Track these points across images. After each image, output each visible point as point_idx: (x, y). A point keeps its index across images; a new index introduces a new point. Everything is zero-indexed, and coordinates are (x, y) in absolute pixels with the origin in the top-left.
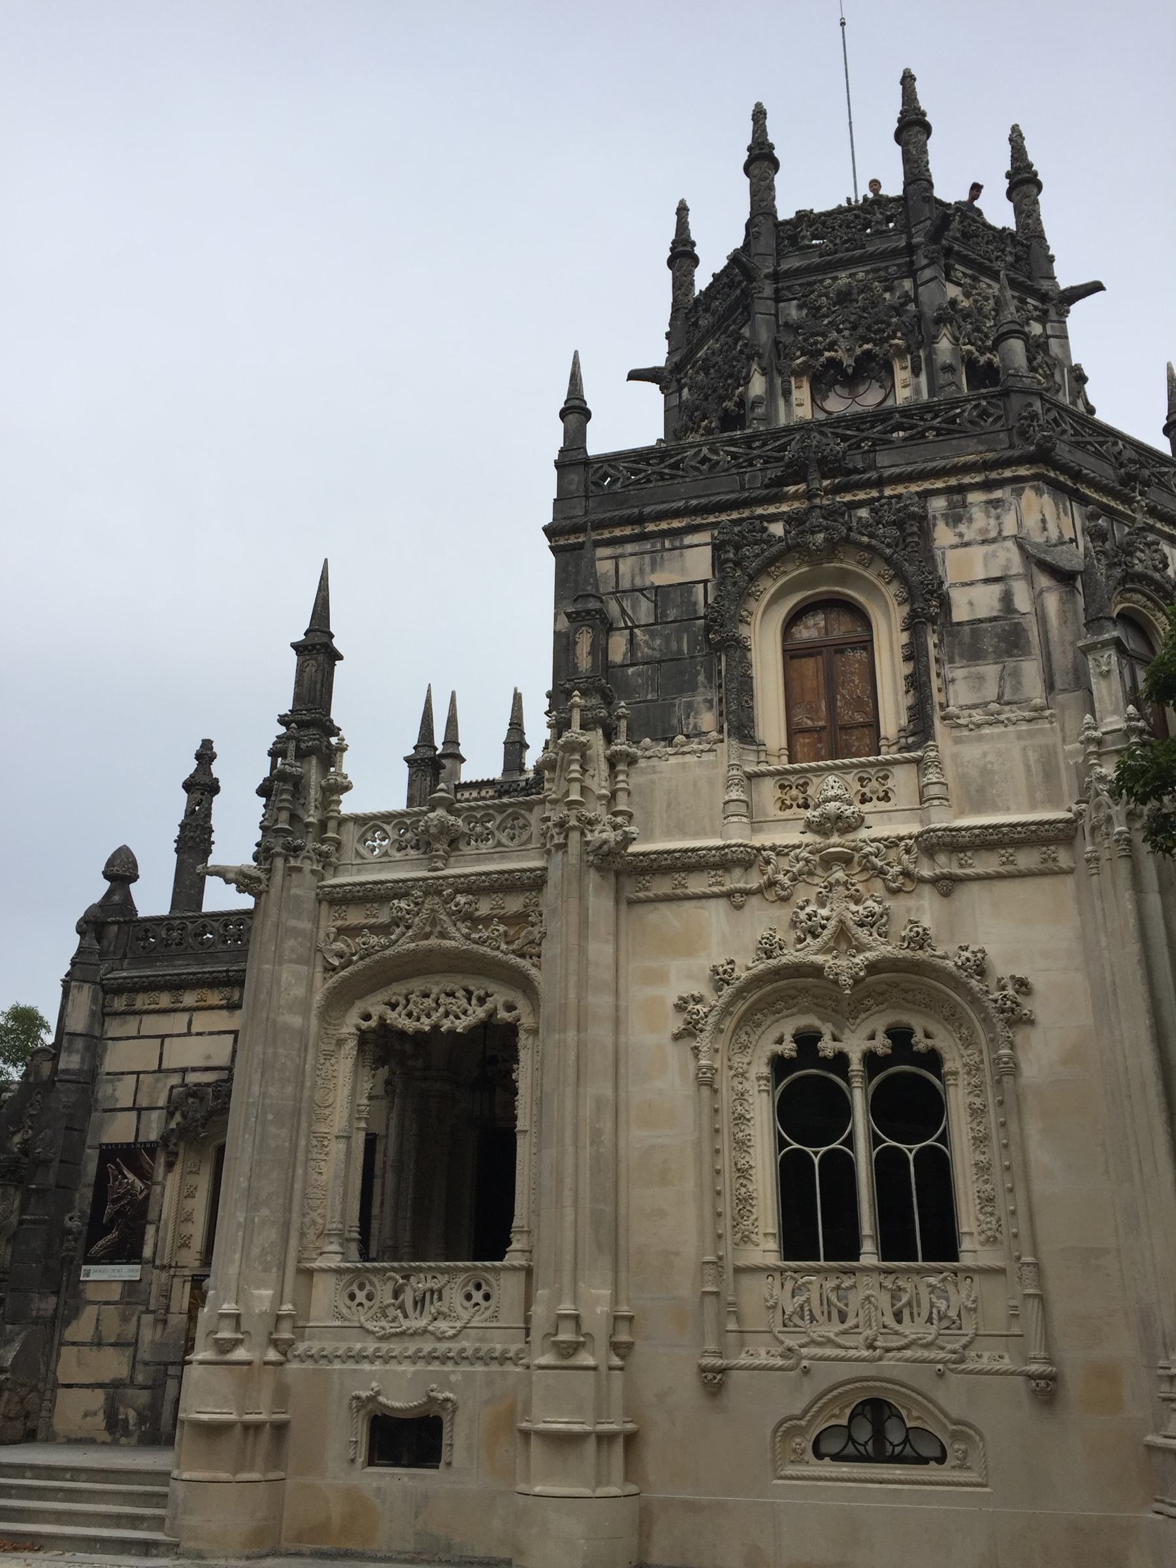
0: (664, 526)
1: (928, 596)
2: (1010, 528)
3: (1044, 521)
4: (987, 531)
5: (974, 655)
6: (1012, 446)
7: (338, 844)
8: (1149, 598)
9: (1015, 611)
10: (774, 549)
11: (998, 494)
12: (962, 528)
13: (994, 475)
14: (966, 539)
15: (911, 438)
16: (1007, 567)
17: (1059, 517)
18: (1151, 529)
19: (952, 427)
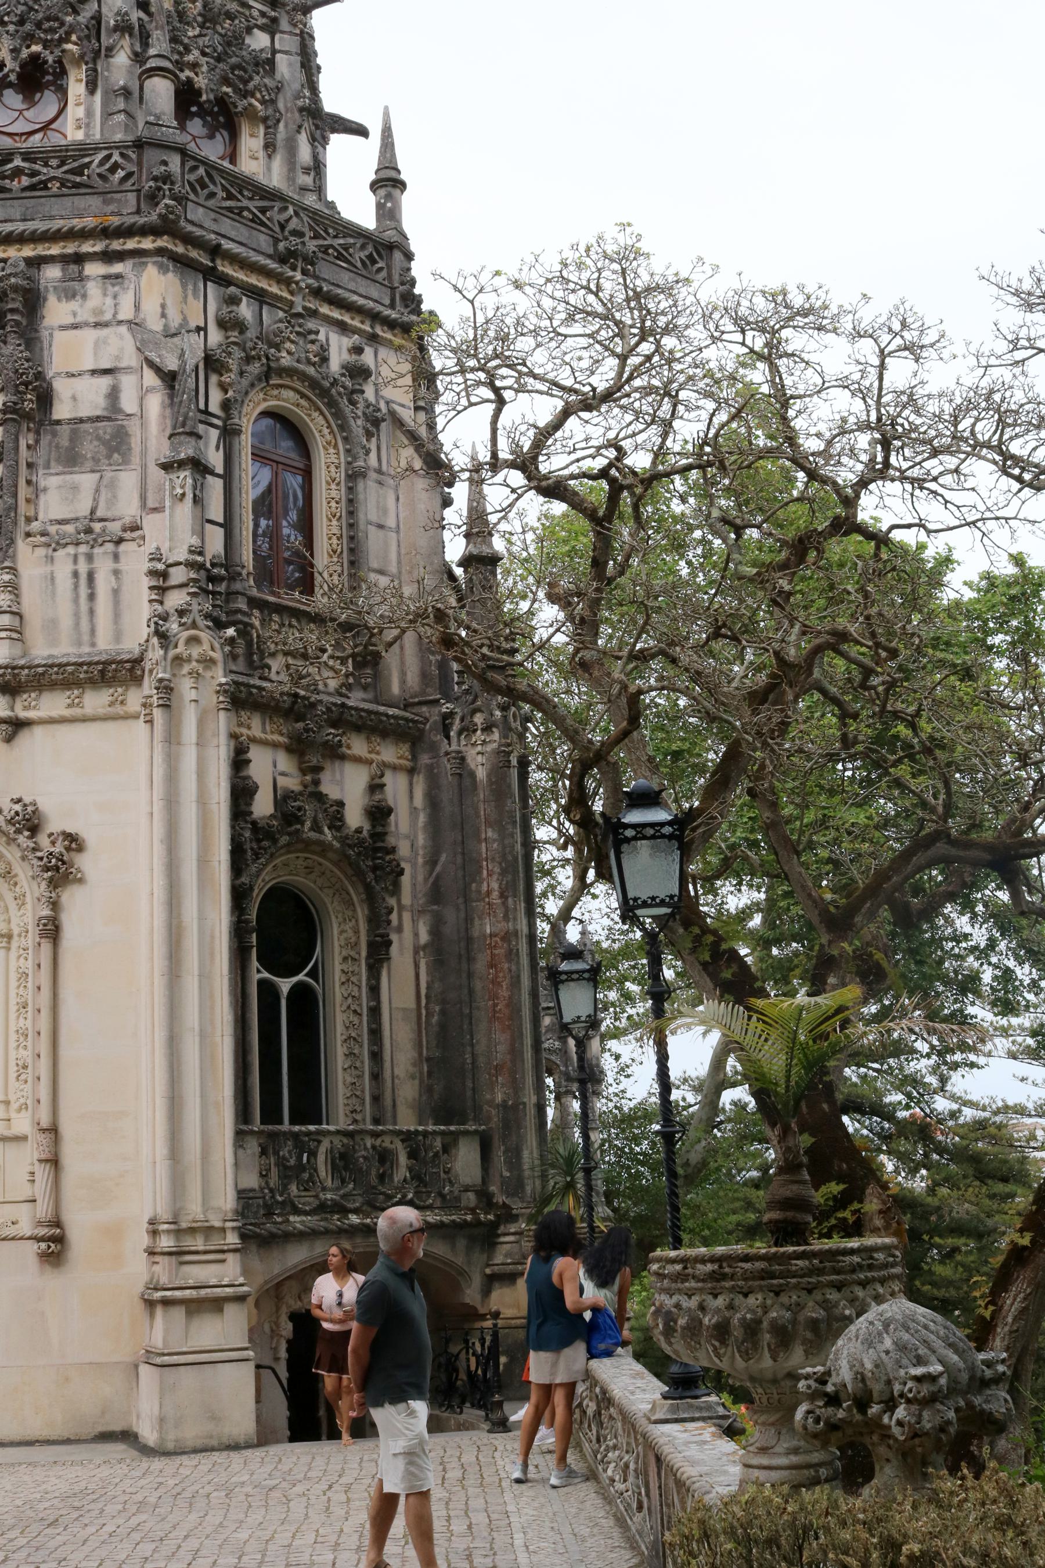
1: (22, 388)
2: (126, 312)
3: (163, 306)
4: (102, 312)
5: (71, 460)
6: (138, 212)
8: (303, 396)
9: (120, 411)
11: (118, 268)
12: (74, 305)
13: (116, 245)
14: (79, 319)
15: (32, 187)
16: (118, 358)
18: (314, 313)
19: (78, 179)
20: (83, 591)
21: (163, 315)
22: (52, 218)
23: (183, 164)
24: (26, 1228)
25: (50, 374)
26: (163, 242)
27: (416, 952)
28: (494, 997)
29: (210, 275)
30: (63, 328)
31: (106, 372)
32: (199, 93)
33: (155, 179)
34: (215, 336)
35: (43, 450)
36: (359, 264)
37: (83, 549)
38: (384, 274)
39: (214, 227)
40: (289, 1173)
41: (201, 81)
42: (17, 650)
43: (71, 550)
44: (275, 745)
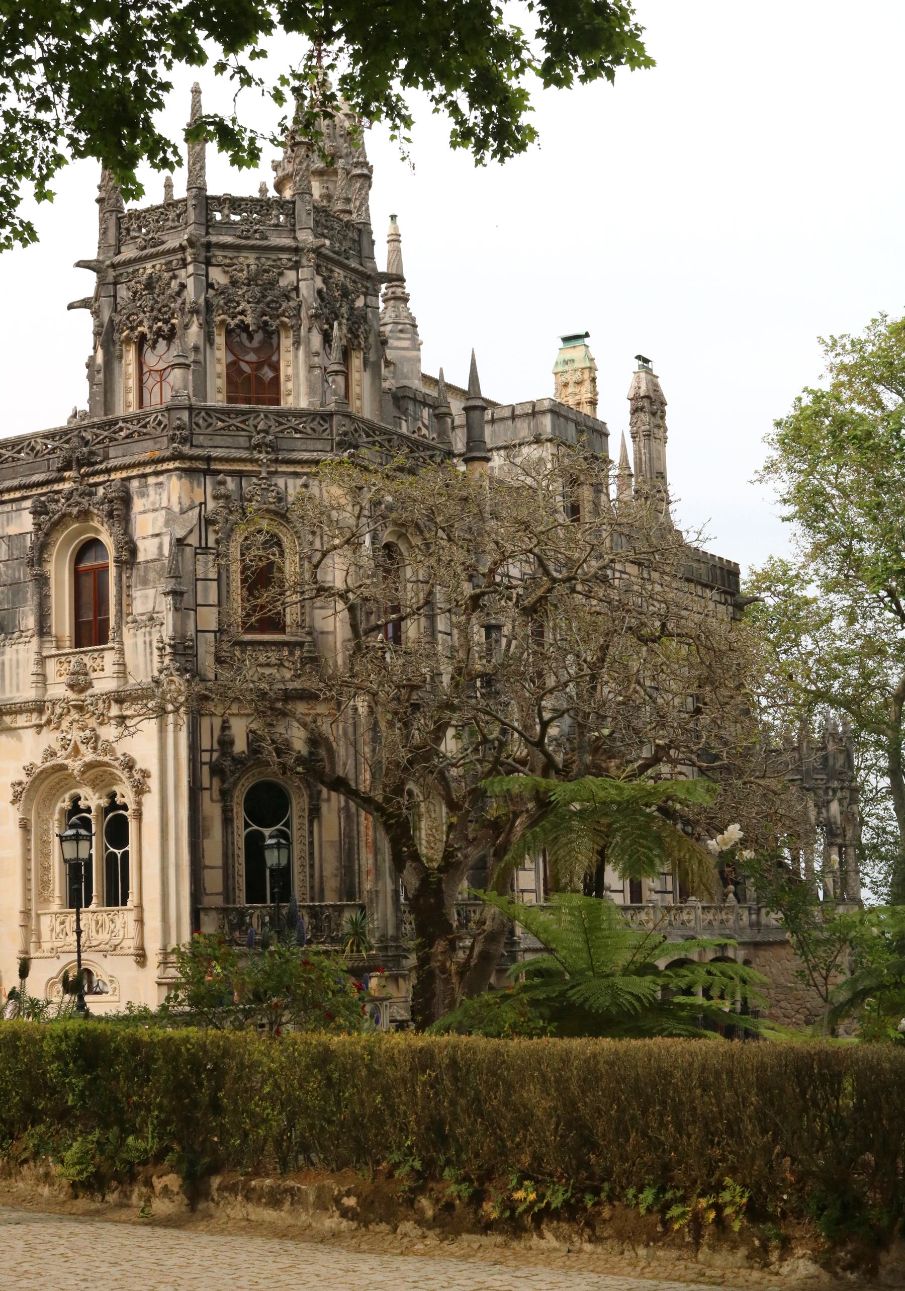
0: (12, 496)
3: (180, 498)
5: (145, 582)
10: (56, 517)
11: (161, 479)
12: (144, 500)
13: (160, 468)
15: (127, 437)
17: (192, 491)
19: (145, 430)
21: (180, 503)
22: (133, 454)
24: (132, 951)
25: (135, 538)
26: (177, 464)
27: (339, 811)
28: (367, 835)
29: (207, 472)
31: (157, 535)
32: (248, 326)
34: (211, 505)
35: (133, 578)
36: (309, 431)
37: (148, 629)
38: (328, 431)
40: (233, 928)
41: (249, 320)
42: (122, 681)
43: (143, 630)
44: (248, 715)
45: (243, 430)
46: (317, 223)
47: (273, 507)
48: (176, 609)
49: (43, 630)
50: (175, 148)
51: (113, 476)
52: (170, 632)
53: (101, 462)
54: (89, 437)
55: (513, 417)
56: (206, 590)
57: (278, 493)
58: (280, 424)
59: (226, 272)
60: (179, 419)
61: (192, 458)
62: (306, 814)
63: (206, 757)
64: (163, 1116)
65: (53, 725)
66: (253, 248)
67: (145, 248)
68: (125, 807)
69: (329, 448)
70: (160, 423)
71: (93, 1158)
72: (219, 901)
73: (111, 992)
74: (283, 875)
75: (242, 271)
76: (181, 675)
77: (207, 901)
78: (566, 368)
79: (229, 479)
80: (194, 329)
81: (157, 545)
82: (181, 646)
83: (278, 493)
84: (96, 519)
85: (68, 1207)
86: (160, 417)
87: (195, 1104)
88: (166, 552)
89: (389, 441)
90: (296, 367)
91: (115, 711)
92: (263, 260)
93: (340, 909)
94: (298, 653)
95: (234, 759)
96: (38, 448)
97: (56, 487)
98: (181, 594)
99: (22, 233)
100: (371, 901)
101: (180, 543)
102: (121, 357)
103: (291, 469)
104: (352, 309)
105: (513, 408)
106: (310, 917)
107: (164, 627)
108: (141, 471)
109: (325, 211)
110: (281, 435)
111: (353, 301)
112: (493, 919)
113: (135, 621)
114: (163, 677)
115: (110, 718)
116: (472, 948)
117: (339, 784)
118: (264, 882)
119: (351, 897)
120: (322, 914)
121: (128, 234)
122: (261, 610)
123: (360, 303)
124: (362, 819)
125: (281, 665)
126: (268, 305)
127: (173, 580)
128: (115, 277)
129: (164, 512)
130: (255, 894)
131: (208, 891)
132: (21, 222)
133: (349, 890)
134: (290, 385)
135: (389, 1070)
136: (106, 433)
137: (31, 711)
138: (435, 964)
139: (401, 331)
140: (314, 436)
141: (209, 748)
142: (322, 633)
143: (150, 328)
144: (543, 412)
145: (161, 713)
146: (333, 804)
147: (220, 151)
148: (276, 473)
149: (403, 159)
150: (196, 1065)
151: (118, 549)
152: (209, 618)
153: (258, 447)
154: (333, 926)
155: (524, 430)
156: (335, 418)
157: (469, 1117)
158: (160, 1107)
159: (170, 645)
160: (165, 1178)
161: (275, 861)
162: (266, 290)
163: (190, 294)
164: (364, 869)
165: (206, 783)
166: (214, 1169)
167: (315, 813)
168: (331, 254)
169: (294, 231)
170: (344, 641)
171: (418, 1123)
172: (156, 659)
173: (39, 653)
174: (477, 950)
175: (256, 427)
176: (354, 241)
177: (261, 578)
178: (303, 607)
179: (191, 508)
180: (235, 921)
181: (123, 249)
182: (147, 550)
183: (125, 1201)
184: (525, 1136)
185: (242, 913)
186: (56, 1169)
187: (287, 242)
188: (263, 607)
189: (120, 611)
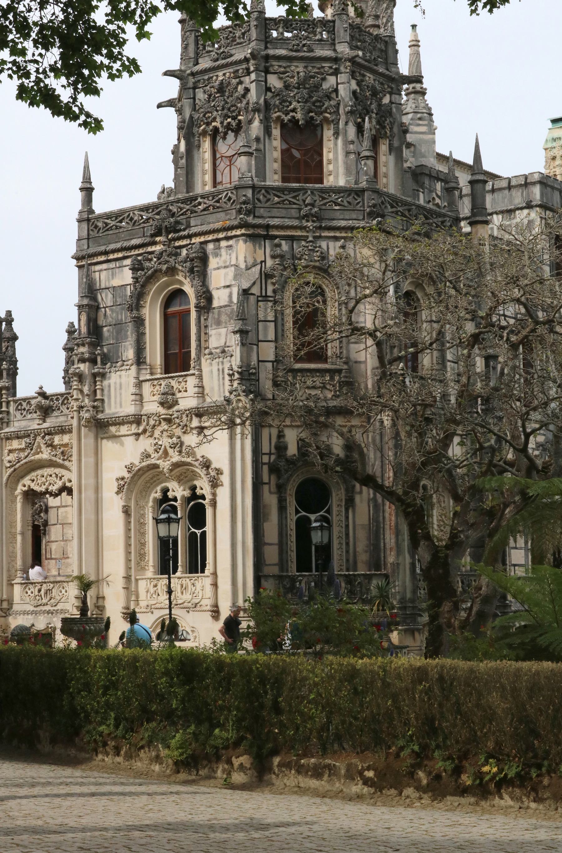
0: (116, 256)
3: (245, 257)
5: (218, 323)
7: (8, 413)
10: (150, 272)
11: (231, 242)
13: (230, 234)
15: (204, 210)
17: (255, 252)
19: (218, 205)
20: (221, 376)
21: (245, 261)
22: (209, 223)
23: (253, 193)
24: (209, 608)
25: (211, 288)
26: (243, 231)
28: (390, 520)
29: (267, 237)
30: (215, 269)
31: (228, 286)
32: (298, 121)
33: (241, 203)
34: (270, 263)
36: (346, 203)
37: (221, 359)
38: (361, 204)
39: (269, 215)
41: (299, 116)
42: (201, 400)
43: (217, 360)
44: (298, 426)
45: (295, 204)
46: (352, 37)
47: (317, 264)
48: (243, 344)
49: (140, 360)
50: (245, 5)
51: (193, 241)
52: (238, 362)
53: (184, 230)
54: (174, 209)
55: (510, 187)
56: (266, 329)
57: (322, 253)
58: (324, 198)
59: (281, 78)
60: (245, 196)
61: (254, 226)
62: (344, 503)
63: (265, 459)
64: (240, 715)
65: (148, 434)
66: (302, 59)
67: (217, 60)
68: (203, 497)
69: (361, 217)
70: (230, 199)
71: (190, 744)
72: (275, 570)
73: (192, 640)
74: (325, 551)
75: (293, 77)
76: (247, 396)
77: (267, 570)
78: (554, 144)
79: (283, 242)
80: (256, 123)
81: (228, 294)
82: (246, 373)
83: (322, 253)
84: (180, 274)
85: (173, 778)
86: (230, 194)
87: (262, 706)
88: (235, 300)
89: (409, 210)
90: (336, 153)
91: (195, 423)
92: (310, 68)
93: (369, 577)
94: (337, 378)
95: (287, 460)
96: (136, 218)
97: (150, 249)
98: (247, 332)
99: (128, 67)
100: (394, 571)
101: (245, 293)
102: (199, 146)
103: (332, 234)
104: (380, 105)
105: (509, 180)
106: (346, 584)
107: (233, 358)
108: (215, 236)
109: (359, 28)
110: (324, 207)
111: (381, 99)
112: (488, 586)
113: (211, 353)
114: (232, 397)
115: (192, 429)
116: (471, 608)
117: (369, 481)
118: (310, 555)
119: (377, 567)
120: (356, 581)
121: (204, 48)
122: (308, 346)
123: (386, 100)
124: (387, 507)
125: (324, 387)
126: (314, 103)
127: (241, 322)
128: (194, 83)
129: (233, 269)
130: (303, 564)
131: (267, 562)
132: (128, 59)
133: (376, 562)
134: (331, 167)
135: (398, 683)
136: (188, 207)
137: (131, 423)
138: (442, 621)
139: (420, 119)
140: (351, 207)
141: (268, 451)
142: (356, 362)
143: (222, 123)
144: (534, 183)
145: (231, 425)
146: (364, 496)
147: (279, 5)
148: (320, 237)
149: (416, 6)
150: (263, 679)
151: (198, 297)
152: (268, 351)
153: (306, 217)
154: (364, 590)
155: (518, 198)
156: (366, 194)
157: (452, 715)
158: (238, 709)
159: (238, 372)
160: (241, 758)
161: (319, 540)
162: (312, 92)
163: (253, 96)
164: (388, 546)
165: (266, 479)
166: (275, 752)
167: (350, 503)
168: (363, 62)
169: (334, 44)
170: (373, 369)
171: (417, 719)
172: (227, 383)
173: (137, 378)
174: (475, 609)
175: (304, 201)
176: (382, 51)
177: (309, 320)
178: (341, 342)
179: (254, 265)
180: (289, 586)
181: (200, 60)
182: (220, 298)
183: (213, 774)
184: (490, 728)
185: (293, 580)
186: (164, 752)
187: (328, 53)
188: (310, 343)
189: (199, 346)
